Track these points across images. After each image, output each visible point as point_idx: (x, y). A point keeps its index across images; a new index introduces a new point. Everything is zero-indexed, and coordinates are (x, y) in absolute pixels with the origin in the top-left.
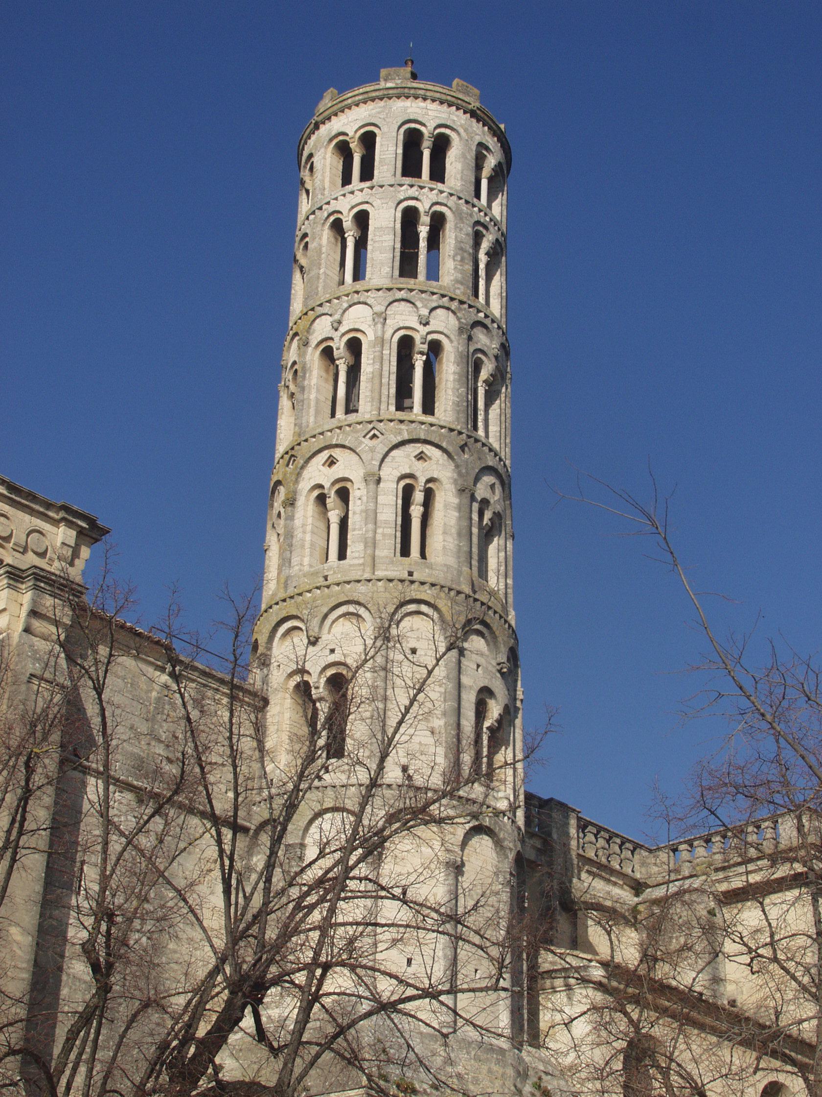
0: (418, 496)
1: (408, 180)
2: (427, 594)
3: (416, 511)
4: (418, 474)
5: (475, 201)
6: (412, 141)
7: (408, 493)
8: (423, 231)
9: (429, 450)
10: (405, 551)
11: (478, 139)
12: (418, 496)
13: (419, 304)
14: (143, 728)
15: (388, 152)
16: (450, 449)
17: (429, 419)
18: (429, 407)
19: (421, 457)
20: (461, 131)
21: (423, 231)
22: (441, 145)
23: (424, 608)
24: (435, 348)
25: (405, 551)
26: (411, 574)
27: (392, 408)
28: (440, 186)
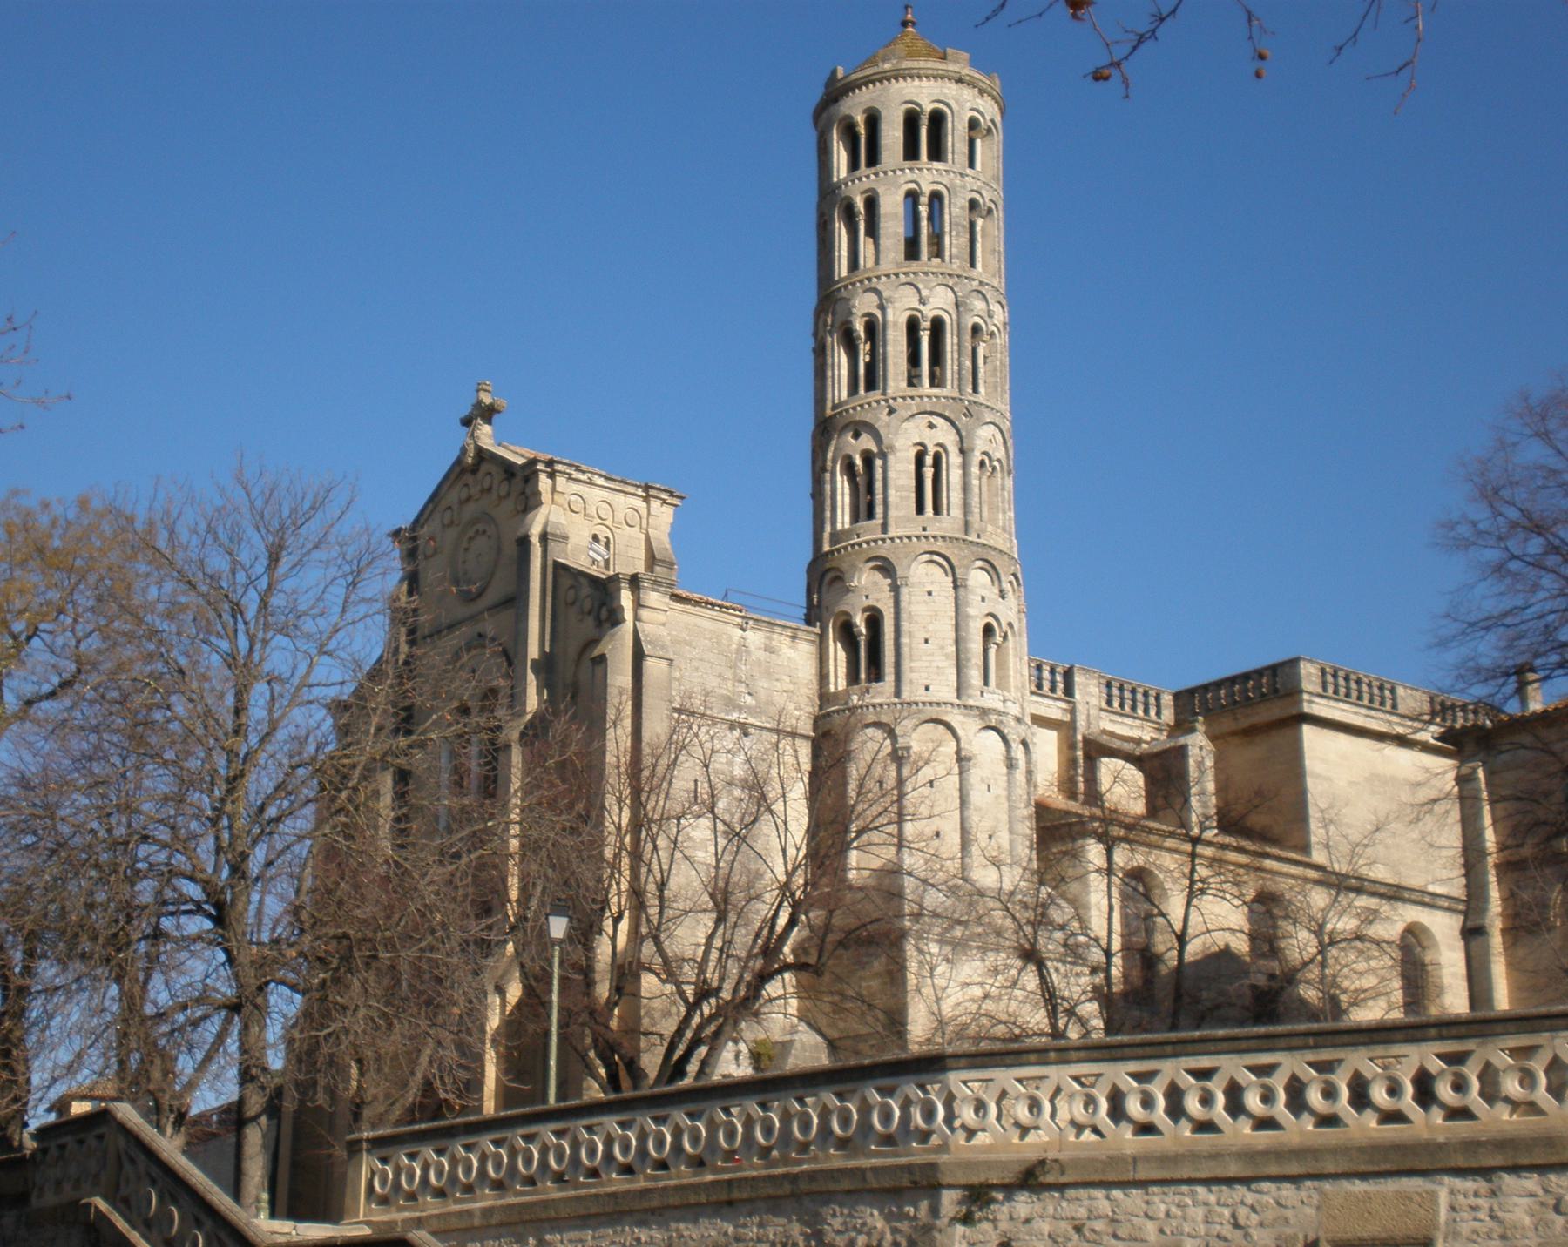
0: (929, 460)
1: (908, 164)
2: (940, 546)
3: (929, 472)
4: (926, 442)
5: (968, 171)
6: (911, 121)
7: (919, 460)
8: (923, 211)
9: (936, 420)
10: (920, 509)
11: (968, 105)
12: (929, 460)
13: (920, 286)
14: (729, 674)
15: (892, 136)
16: (952, 417)
17: (936, 391)
18: (936, 381)
19: (931, 426)
20: (952, 103)
21: (923, 211)
22: (937, 119)
23: (936, 558)
24: (937, 326)
25: (920, 509)
26: (924, 529)
27: (904, 384)
28: (936, 165)
